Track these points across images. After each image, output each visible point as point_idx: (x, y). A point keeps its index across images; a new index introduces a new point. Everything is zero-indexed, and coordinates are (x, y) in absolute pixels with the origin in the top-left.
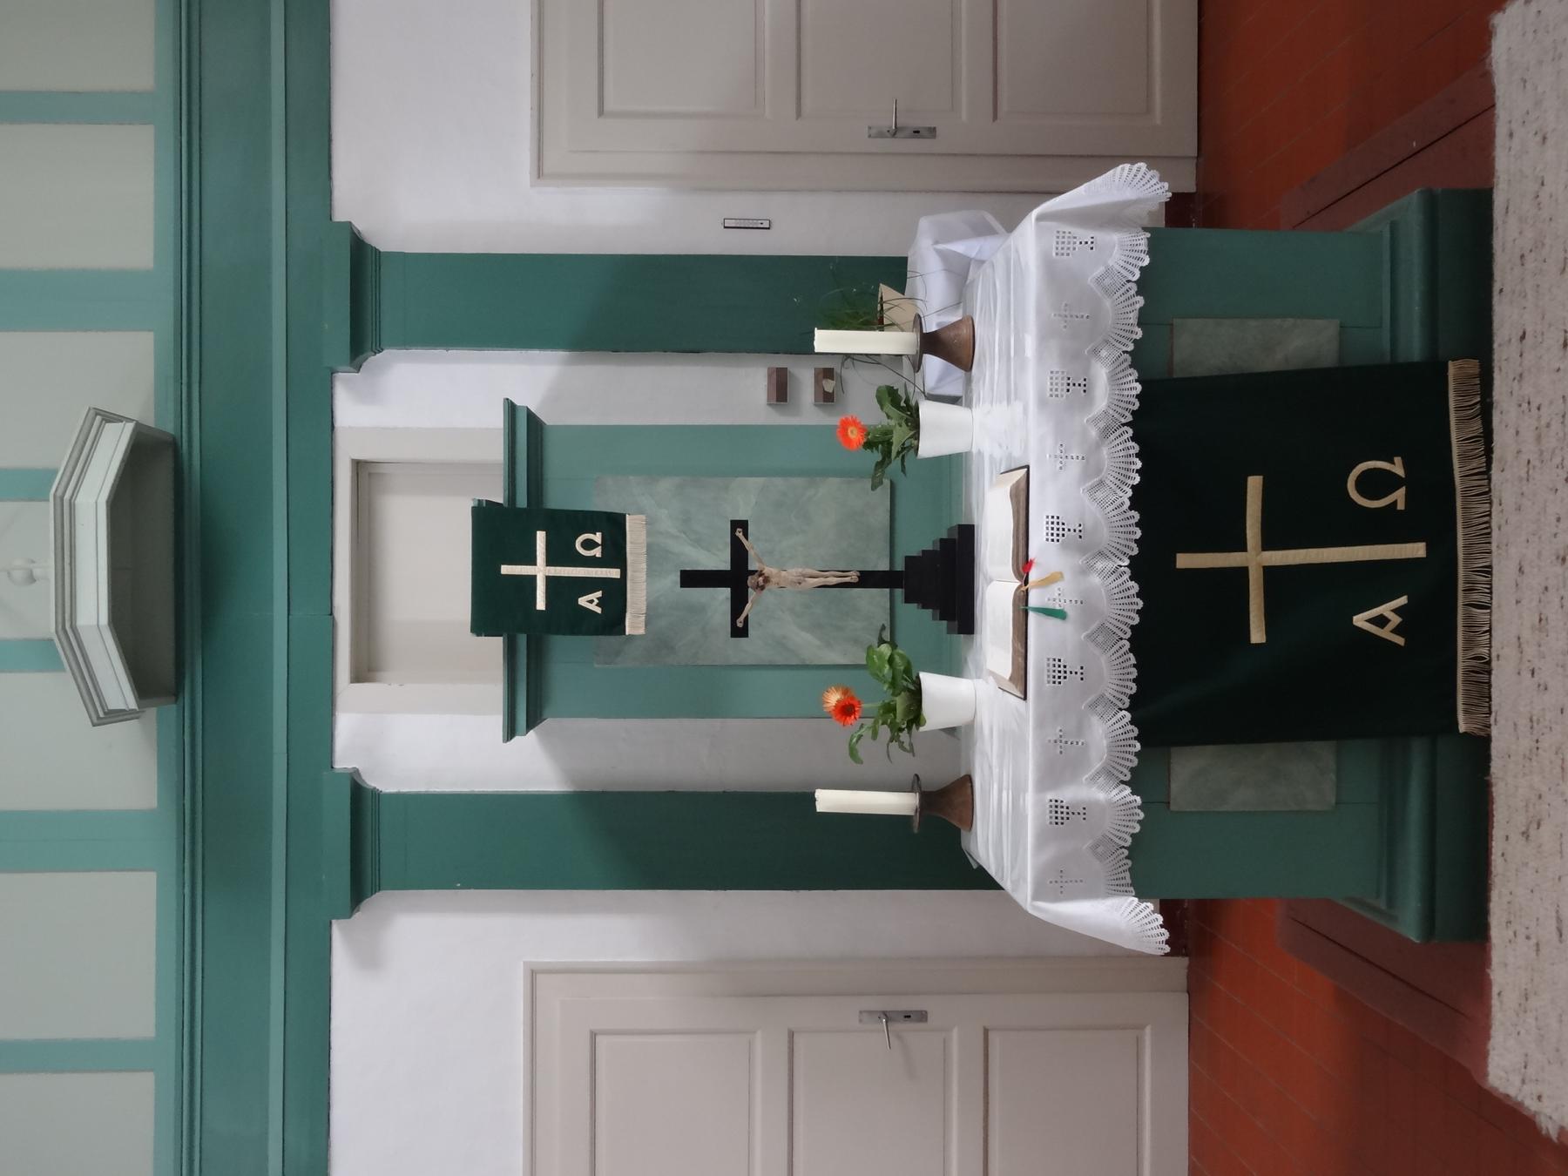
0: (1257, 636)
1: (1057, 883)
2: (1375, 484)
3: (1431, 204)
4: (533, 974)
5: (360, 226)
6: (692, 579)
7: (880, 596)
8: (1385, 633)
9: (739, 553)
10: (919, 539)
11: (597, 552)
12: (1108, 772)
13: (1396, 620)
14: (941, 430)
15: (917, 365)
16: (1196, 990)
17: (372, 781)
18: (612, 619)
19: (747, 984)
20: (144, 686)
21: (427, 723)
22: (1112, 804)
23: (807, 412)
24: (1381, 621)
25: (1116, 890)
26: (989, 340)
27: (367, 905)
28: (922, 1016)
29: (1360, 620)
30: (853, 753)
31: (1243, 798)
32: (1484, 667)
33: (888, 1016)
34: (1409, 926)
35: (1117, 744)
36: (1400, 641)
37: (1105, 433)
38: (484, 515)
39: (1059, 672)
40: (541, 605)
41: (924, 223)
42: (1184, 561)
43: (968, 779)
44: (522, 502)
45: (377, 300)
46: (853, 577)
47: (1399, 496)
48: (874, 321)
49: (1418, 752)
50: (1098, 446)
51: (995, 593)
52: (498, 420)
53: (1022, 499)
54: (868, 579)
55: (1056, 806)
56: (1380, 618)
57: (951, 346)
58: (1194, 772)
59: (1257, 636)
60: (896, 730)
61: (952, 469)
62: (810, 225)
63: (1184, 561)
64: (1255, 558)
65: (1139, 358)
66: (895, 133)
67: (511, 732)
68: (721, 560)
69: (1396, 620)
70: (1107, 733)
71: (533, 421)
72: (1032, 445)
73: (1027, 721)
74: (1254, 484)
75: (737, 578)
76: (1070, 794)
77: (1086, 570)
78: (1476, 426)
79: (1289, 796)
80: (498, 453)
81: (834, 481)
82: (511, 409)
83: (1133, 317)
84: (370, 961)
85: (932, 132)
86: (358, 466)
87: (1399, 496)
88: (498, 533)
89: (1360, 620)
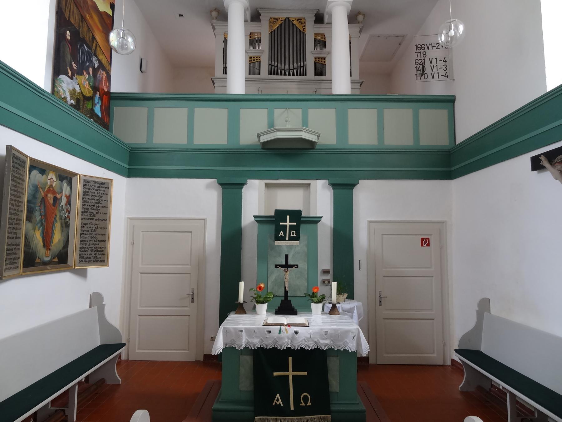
0: (275, 374)
1: (226, 332)
2: (305, 398)
3: (363, 412)
4: (204, 220)
5: (358, 185)
6: (287, 257)
7: (283, 294)
8: (275, 401)
9: (292, 266)
10: (294, 302)
11: (292, 235)
12: (248, 342)
13: (278, 403)
14: (316, 308)
15: (329, 303)
16: (196, 362)
17: (244, 187)
19: (200, 264)
20: (264, 143)
21: (256, 199)
22: (242, 344)
23: (321, 278)
24: (278, 400)
25: (224, 344)
26: (335, 318)
27: (220, 188)
28: (193, 302)
29: (278, 396)
30: (251, 289)
31: (242, 371)
33: (193, 295)
34: (216, 406)
35: (254, 344)
36: (274, 404)
37: (316, 342)
38: (299, 212)
39: (268, 332)
40: (281, 224)
41: (361, 303)
42: (290, 359)
43: (245, 313)
44: (302, 219)
45: (343, 189)
46: (287, 289)
47: (303, 404)
49: (252, 408)
50: (313, 341)
51: (284, 319)
52: (318, 215)
53: (303, 325)
54: (286, 292)
55: (242, 332)
56: (278, 400)
57: (334, 310)
58: (248, 360)
59: (275, 374)
60: (256, 298)
61: (308, 310)
63: (290, 359)
64: (291, 374)
65: (331, 349)
66: (380, 297)
67: (255, 217)
68: (291, 262)
69: (278, 403)
70: (256, 343)
71: (317, 222)
72: (313, 327)
73: (256, 325)
74: (305, 373)
75: (287, 266)
76: (244, 334)
77: (288, 338)
79: (242, 381)
80: (312, 214)
82: (321, 217)
83: (339, 348)
84: (208, 187)
85: (380, 305)
86: (310, 184)
87: (303, 404)
88: (296, 215)
89: (278, 396)
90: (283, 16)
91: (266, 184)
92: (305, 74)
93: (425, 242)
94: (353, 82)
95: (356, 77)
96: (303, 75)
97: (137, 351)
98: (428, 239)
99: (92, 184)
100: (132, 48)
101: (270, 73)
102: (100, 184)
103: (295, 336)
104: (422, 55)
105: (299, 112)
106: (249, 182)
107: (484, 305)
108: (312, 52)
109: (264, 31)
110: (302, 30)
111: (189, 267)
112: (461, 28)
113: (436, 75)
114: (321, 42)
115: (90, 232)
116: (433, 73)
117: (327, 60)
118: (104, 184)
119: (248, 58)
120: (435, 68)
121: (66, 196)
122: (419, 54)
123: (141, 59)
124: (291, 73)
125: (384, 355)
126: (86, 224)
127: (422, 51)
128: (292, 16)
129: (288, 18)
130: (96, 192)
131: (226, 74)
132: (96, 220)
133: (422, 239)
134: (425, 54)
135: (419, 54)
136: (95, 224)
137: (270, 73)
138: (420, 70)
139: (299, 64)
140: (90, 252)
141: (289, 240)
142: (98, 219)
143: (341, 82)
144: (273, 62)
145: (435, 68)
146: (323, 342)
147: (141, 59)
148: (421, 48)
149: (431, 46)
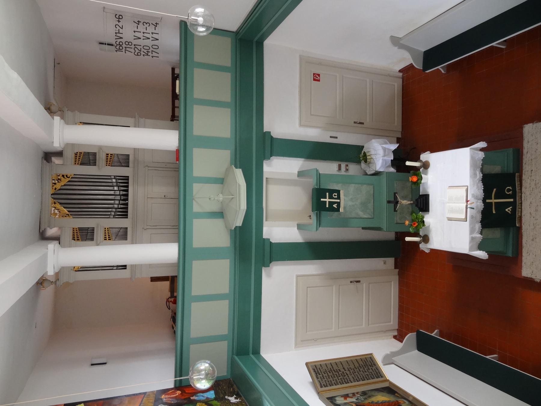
0: (494, 212)
4: (298, 276)
8: (509, 212)
9: (395, 197)
18: (338, 210)
19: (333, 277)
23: (343, 172)
24: (509, 210)
29: (507, 210)
32: (521, 217)
39: (472, 217)
40: (327, 206)
47: (511, 192)
48: (416, 161)
56: (509, 210)
62: (345, 138)
65: (482, 170)
70: (478, 226)
74: (495, 189)
77: (477, 202)
78: (519, 183)
81: (365, 185)
84: (269, 275)
89: (507, 210)
90: (49, 200)
92: (127, 178)
93: (316, 78)
95: (130, 121)
96: (128, 179)
97: (392, 323)
98: (314, 74)
99: (320, 379)
100: (207, 365)
101: (125, 215)
102: (316, 374)
103: (476, 198)
104: (128, 46)
105: (196, 187)
106: (265, 236)
107: (396, 41)
110: (68, 179)
111: (334, 287)
112: (200, 10)
114: (87, 158)
115: (357, 373)
116: (151, 39)
117: (110, 152)
118: (314, 369)
120: (145, 35)
121: (345, 399)
122: (127, 49)
123: (92, 365)
124: (124, 193)
125: (396, 124)
126: (354, 378)
127: (124, 46)
128: (49, 190)
130: (324, 375)
131: (126, 266)
132: (345, 370)
133: (314, 80)
135: (127, 49)
136: (349, 370)
137: (125, 215)
138: (148, 52)
139: (115, 184)
140: (371, 371)
141: (340, 199)
142: (344, 369)
143: (166, 139)
144: (113, 213)
145: (145, 35)
146: (478, 177)
147: (92, 365)
148: (121, 46)
149: (118, 35)
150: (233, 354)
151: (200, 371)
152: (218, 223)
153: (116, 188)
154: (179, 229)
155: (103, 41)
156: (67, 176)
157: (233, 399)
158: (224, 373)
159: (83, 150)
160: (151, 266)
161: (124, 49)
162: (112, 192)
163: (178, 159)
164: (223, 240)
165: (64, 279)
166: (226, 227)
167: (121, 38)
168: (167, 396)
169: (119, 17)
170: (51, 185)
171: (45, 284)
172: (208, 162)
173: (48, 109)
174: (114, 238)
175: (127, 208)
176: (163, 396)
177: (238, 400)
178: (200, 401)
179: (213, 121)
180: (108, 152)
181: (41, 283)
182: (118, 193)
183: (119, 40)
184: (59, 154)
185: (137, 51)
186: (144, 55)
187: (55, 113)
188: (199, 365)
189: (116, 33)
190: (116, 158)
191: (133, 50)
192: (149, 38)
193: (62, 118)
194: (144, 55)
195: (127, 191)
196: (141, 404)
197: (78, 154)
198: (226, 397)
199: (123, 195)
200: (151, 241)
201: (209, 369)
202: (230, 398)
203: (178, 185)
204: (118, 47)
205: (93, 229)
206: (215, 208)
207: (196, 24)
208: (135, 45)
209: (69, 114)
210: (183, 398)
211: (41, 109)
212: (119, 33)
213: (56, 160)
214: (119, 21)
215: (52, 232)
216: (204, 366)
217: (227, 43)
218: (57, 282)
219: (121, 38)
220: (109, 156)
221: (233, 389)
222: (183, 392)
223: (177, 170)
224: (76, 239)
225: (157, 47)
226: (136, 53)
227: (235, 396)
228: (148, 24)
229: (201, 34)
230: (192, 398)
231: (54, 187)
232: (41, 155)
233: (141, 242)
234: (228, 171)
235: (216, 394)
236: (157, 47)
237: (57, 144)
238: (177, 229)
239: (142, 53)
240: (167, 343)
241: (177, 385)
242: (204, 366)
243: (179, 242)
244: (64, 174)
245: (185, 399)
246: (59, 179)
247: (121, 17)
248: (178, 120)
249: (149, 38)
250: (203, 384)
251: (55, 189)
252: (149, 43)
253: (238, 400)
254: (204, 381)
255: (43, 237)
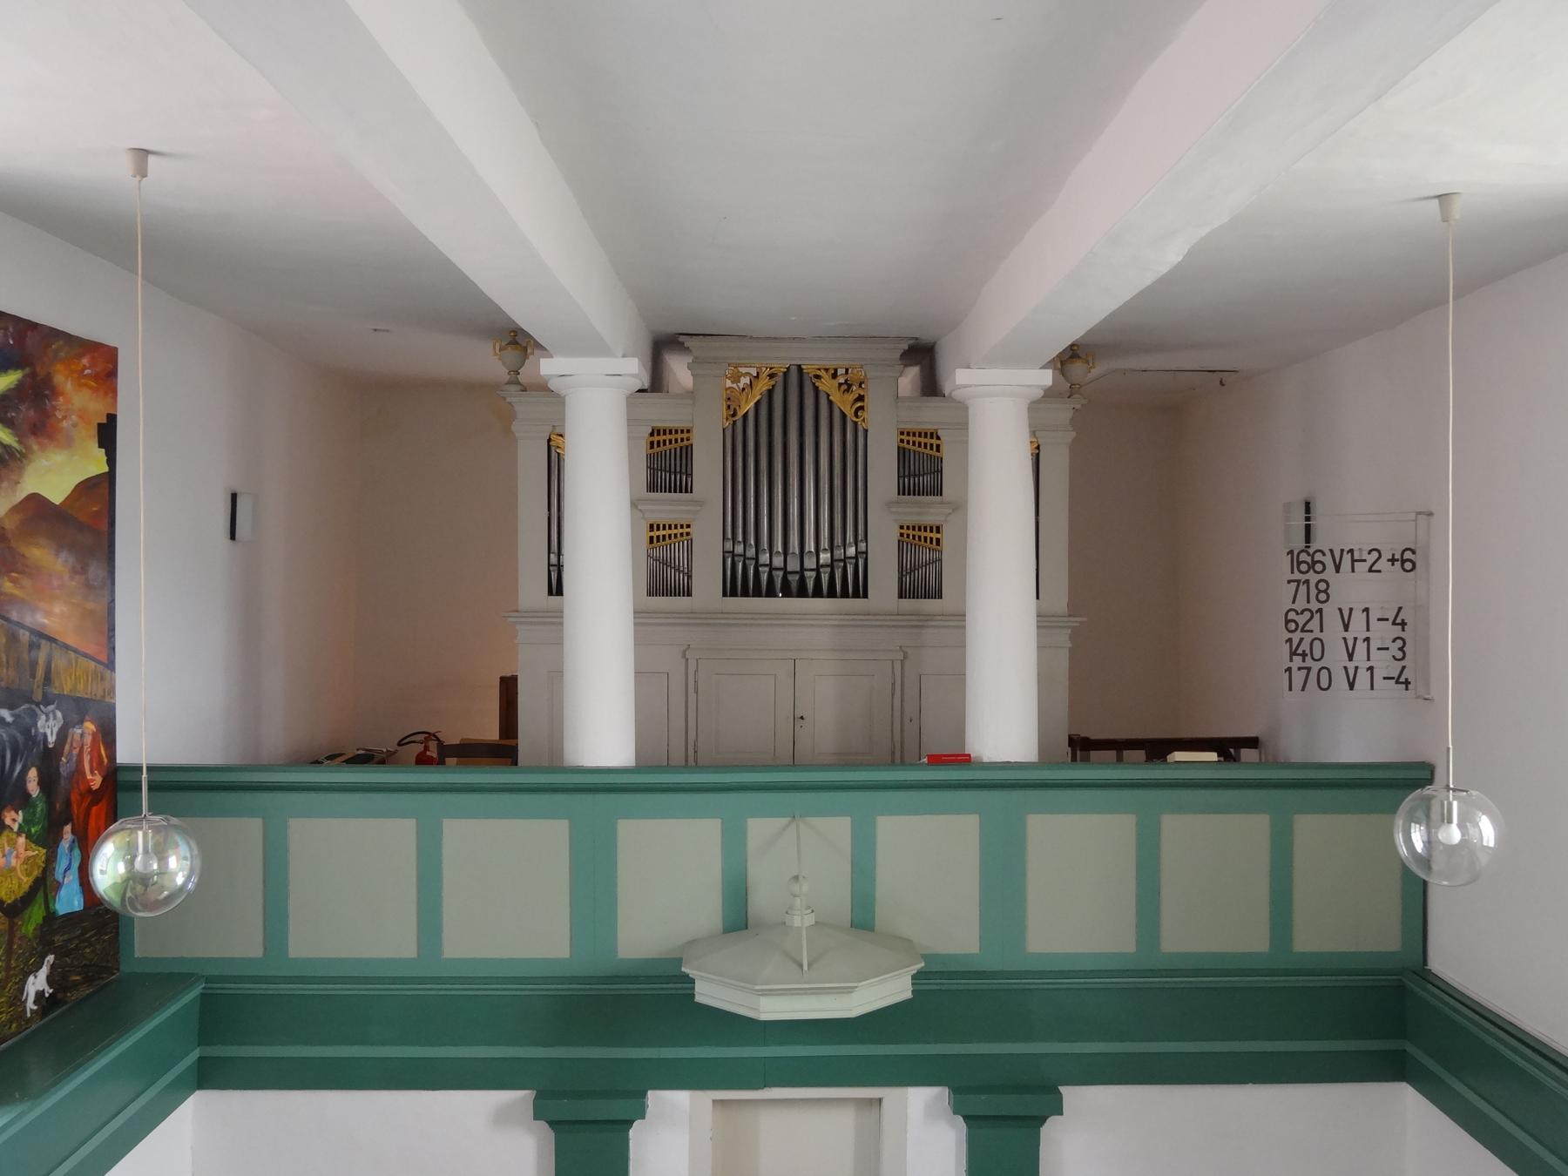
84: (501, 1118)
86: (880, 1100)
90: (782, 359)
91: (715, 1102)
92: (861, 591)
94: (1045, 621)
95: (1059, 601)
96: (856, 595)
101: (733, 588)
104: (1313, 592)
106: (655, 1098)
108: (889, 504)
109: (702, 410)
110: (850, 413)
112: (1487, 831)
113: (1363, 678)
114: (923, 467)
116: (1351, 666)
117: (946, 537)
119: (646, 527)
120: (1361, 648)
122: (1303, 588)
123: (234, 497)
124: (810, 584)
127: (1313, 577)
128: (812, 360)
129: (799, 366)
131: (560, 592)
134: (1324, 591)
135: (1303, 588)
137: (733, 588)
138: (1304, 655)
139: (839, 553)
143: (1004, 718)
144: (739, 549)
147: (234, 497)
148: (1311, 566)
149: (1347, 558)
150: (209, 979)
151: (161, 854)
152: (707, 912)
153: (825, 557)
154: (686, 767)
155: (1318, 510)
156: (862, 408)
157: (37, 983)
158: (146, 946)
159: (947, 454)
160: (556, 677)
161: (1303, 577)
162: (810, 545)
163: (936, 760)
164: (641, 933)
165: (525, 407)
166: (691, 943)
167: (1338, 569)
168: (88, 739)
169: (1406, 561)
170: (831, 364)
171: (511, 354)
172: (930, 867)
173: (1071, 356)
174: (656, 553)
175: (757, 593)
176: (90, 727)
177: (30, 1005)
178: (51, 859)
179: (1085, 886)
180: (945, 529)
181: (518, 342)
182: (810, 563)
183: (1328, 560)
184: (931, 387)
185: (1301, 620)
186: (1290, 640)
187: (1063, 372)
188: (183, 849)
189: (1351, 551)
190: (926, 556)
191: (1301, 604)
192: (1351, 657)
193: (1050, 394)
194: (1290, 640)
195: (818, 593)
196: (76, 651)
197: (934, 442)
198: (51, 958)
199: (802, 580)
200: (641, 674)
201: (162, 888)
202: (43, 973)
203: (845, 760)
204: (1303, 557)
205: (688, 489)
206: (762, 900)
207: (1431, 817)
208: (1320, 611)
209: (1063, 413)
210: (74, 797)
211: (1074, 331)
212: (1353, 561)
213: (909, 379)
214: (1393, 560)
215: (679, 370)
216: (178, 868)
217: (1378, 936)
218: (513, 388)
219: (1338, 569)
220: (934, 535)
221: (76, 985)
222: (95, 796)
223: (897, 758)
224: (656, 438)
225: (1324, 684)
226: (1292, 615)
227: (48, 991)
228: (1400, 655)
229: (1399, 838)
230: (68, 828)
231: (822, 373)
232: (926, 336)
233: (640, 642)
234: (903, 945)
235: (71, 917)
236: (1324, 684)
237: (960, 378)
238: (683, 765)
239: (1296, 637)
240: (278, 733)
241: (122, 777)
242: (178, 868)
243: (638, 769)
244: (867, 402)
245: (68, 804)
246: (850, 386)
247: (1408, 566)
248: (1074, 759)
249: (1351, 657)
250: (109, 867)
251: (818, 377)
252: (1335, 657)
253: (30, 1005)
254: (122, 868)
255: (662, 346)
